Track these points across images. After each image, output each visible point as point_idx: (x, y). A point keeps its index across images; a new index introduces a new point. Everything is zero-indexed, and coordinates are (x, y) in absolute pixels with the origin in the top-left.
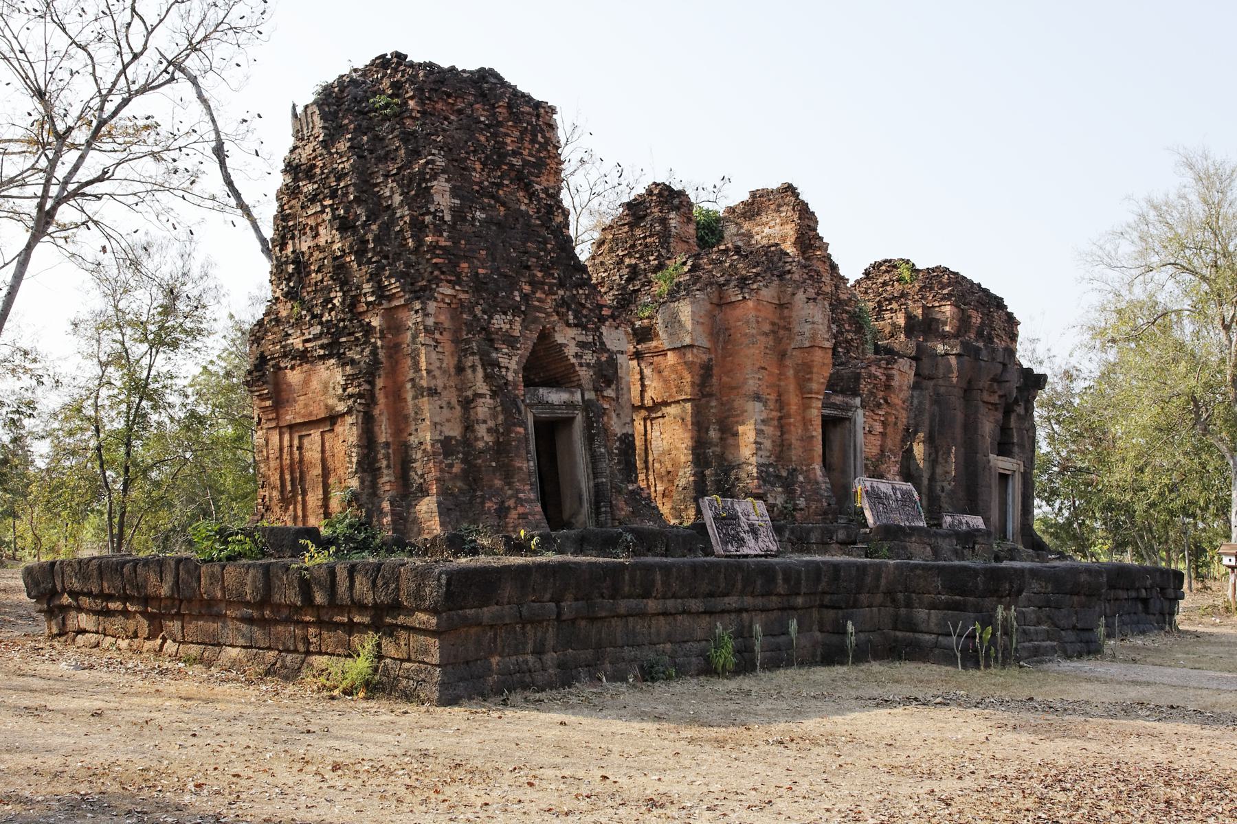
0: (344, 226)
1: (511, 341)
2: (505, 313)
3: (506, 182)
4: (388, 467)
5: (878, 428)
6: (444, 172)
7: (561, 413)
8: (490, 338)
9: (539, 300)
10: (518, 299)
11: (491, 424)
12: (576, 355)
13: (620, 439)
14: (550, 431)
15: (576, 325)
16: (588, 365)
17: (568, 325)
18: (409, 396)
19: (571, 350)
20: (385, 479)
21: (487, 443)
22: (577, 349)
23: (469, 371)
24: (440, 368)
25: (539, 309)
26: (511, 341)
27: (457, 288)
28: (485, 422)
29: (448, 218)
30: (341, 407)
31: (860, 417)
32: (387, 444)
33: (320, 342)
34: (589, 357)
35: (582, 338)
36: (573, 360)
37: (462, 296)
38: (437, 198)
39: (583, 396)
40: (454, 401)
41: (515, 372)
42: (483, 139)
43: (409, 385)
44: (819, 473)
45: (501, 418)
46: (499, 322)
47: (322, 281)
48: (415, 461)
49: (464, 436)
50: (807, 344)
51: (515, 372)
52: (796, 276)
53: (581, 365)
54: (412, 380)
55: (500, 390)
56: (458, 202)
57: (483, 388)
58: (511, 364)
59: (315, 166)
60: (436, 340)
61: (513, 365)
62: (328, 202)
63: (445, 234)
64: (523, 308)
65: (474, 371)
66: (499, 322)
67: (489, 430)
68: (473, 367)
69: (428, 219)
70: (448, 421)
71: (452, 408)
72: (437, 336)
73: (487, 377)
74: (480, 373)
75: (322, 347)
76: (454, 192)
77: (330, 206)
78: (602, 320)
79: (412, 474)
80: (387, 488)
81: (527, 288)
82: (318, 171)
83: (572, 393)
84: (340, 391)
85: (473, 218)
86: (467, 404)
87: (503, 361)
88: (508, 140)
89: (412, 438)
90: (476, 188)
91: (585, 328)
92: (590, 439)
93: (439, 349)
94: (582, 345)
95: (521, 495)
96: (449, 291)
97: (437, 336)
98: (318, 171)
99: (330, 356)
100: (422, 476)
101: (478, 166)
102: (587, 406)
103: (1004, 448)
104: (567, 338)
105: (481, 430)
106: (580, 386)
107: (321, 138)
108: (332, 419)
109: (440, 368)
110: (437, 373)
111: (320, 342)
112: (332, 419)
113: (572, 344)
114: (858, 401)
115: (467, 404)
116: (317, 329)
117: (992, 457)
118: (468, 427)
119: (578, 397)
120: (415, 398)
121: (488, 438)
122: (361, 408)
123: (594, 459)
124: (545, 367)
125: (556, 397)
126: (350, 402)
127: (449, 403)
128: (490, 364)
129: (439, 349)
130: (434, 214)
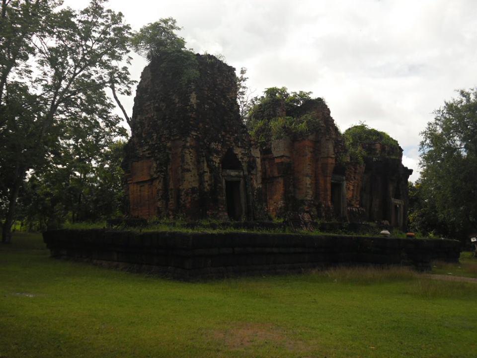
0: (158, 109)
1: (217, 152)
2: (216, 142)
3: (217, 95)
4: (172, 198)
5: (351, 188)
6: (194, 90)
7: (235, 179)
8: (210, 151)
9: (228, 138)
10: (220, 137)
11: (209, 182)
12: (241, 158)
13: (257, 189)
14: (232, 186)
15: (241, 147)
16: (245, 162)
17: (238, 147)
18: (180, 172)
19: (240, 156)
20: (170, 202)
21: (208, 189)
22: (241, 156)
23: (202, 163)
24: (191, 162)
25: (228, 141)
26: (217, 152)
27: (198, 132)
28: (207, 182)
29: (195, 107)
30: (155, 176)
31: (345, 183)
32: (172, 189)
33: (148, 152)
34: (246, 159)
35: (243, 152)
36: (240, 160)
37: (200, 135)
38: (191, 100)
39: (243, 173)
40: (196, 174)
41: (219, 163)
42: (208, 79)
43: (180, 168)
44: (330, 203)
45: (213, 181)
46: (213, 145)
47: (149, 130)
48: (181, 196)
49: (199, 186)
50: (326, 156)
51: (219, 163)
52: (323, 131)
53: (243, 162)
54: (181, 166)
55: (212, 169)
56: (198, 101)
57: (206, 169)
58: (217, 160)
59: (148, 89)
60: (190, 151)
61: (218, 161)
62: (153, 101)
63: (194, 113)
64: (222, 140)
65: (203, 163)
66: (213, 145)
67: (208, 185)
68: (203, 161)
69: (188, 107)
70: (194, 181)
71: (196, 177)
72: (191, 150)
73: (208, 166)
74: (205, 164)
75: (149, 154)
76: (197, 98)
77: (153, 103)
78: (251, 145)
79: (180, 200)
80: (171, 205)
81: (223, 133)
82: (149, 90)
83: (239, 172)
84: (155, 170)
85: (205, 107)
86: (201, 175)
88: (218, 80)
89: (181, 187)
90: (206, 96)
91: (245, 148)
92: (246, 189)
93: (191, 155)
94: (242, 154)
95: (220, 209)
96: (196, 134)
97: (191, 150)
98: (149, 90)
99: (152, 157)
100: (184, 201)
101: (206, 89)
102: (245, 177)
103: (397, 196)
104: (238, 151)
105: (206, 185)
106: (243, 170)
107: (151, 78)
108: (152, 180)
109: (191, 162)
110: (190, 163)
111: (148, 152)
112: (152, 180)
113: (240, 153)
114: (344, 178)
115: (201, 175)
116: (146, 148)
117: (393, 199)
118: (201, 182)
119: (242, 174)
120: (182, 172)
121: (208, 188)
122: (162, 176)
123: (247, 197)
124: (230, 161)
125: (233, 173)
126: (159, 174)
127: (194, 175)
128: (209, 161)
129: (191, 155)
130: (190, 106)
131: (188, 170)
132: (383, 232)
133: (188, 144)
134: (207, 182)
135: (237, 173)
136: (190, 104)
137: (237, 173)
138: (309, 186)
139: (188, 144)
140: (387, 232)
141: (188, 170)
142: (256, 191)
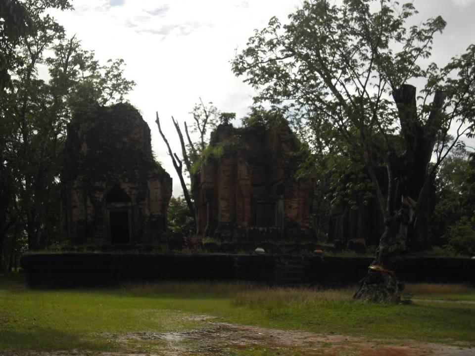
1: (101, 189)
5: (295, 205)
12: (129, 192)
19: (127, 190)
26: (101, 189)
28: (90, 214)
31: (281, 203)
36: (127, 193)
38: (82, 149)
46: (97, 184)
53: (131, 194)
58: (100, 196)
61: (102, 196)
66: (97, 184)
87: (97, 196)
94: (131, 188)
105: (89, 217)
114: (282, 197)
131: (75, 207)
132: (258, 249)
133: (75, 186)
134: (90, 214)
135: (123, 205)
136: (81, 152)
137: (123, 205)
138: (225, 209)
139: (75, 186)
140: (262, 250)
141: (75, 207)
142: (148, 219)
